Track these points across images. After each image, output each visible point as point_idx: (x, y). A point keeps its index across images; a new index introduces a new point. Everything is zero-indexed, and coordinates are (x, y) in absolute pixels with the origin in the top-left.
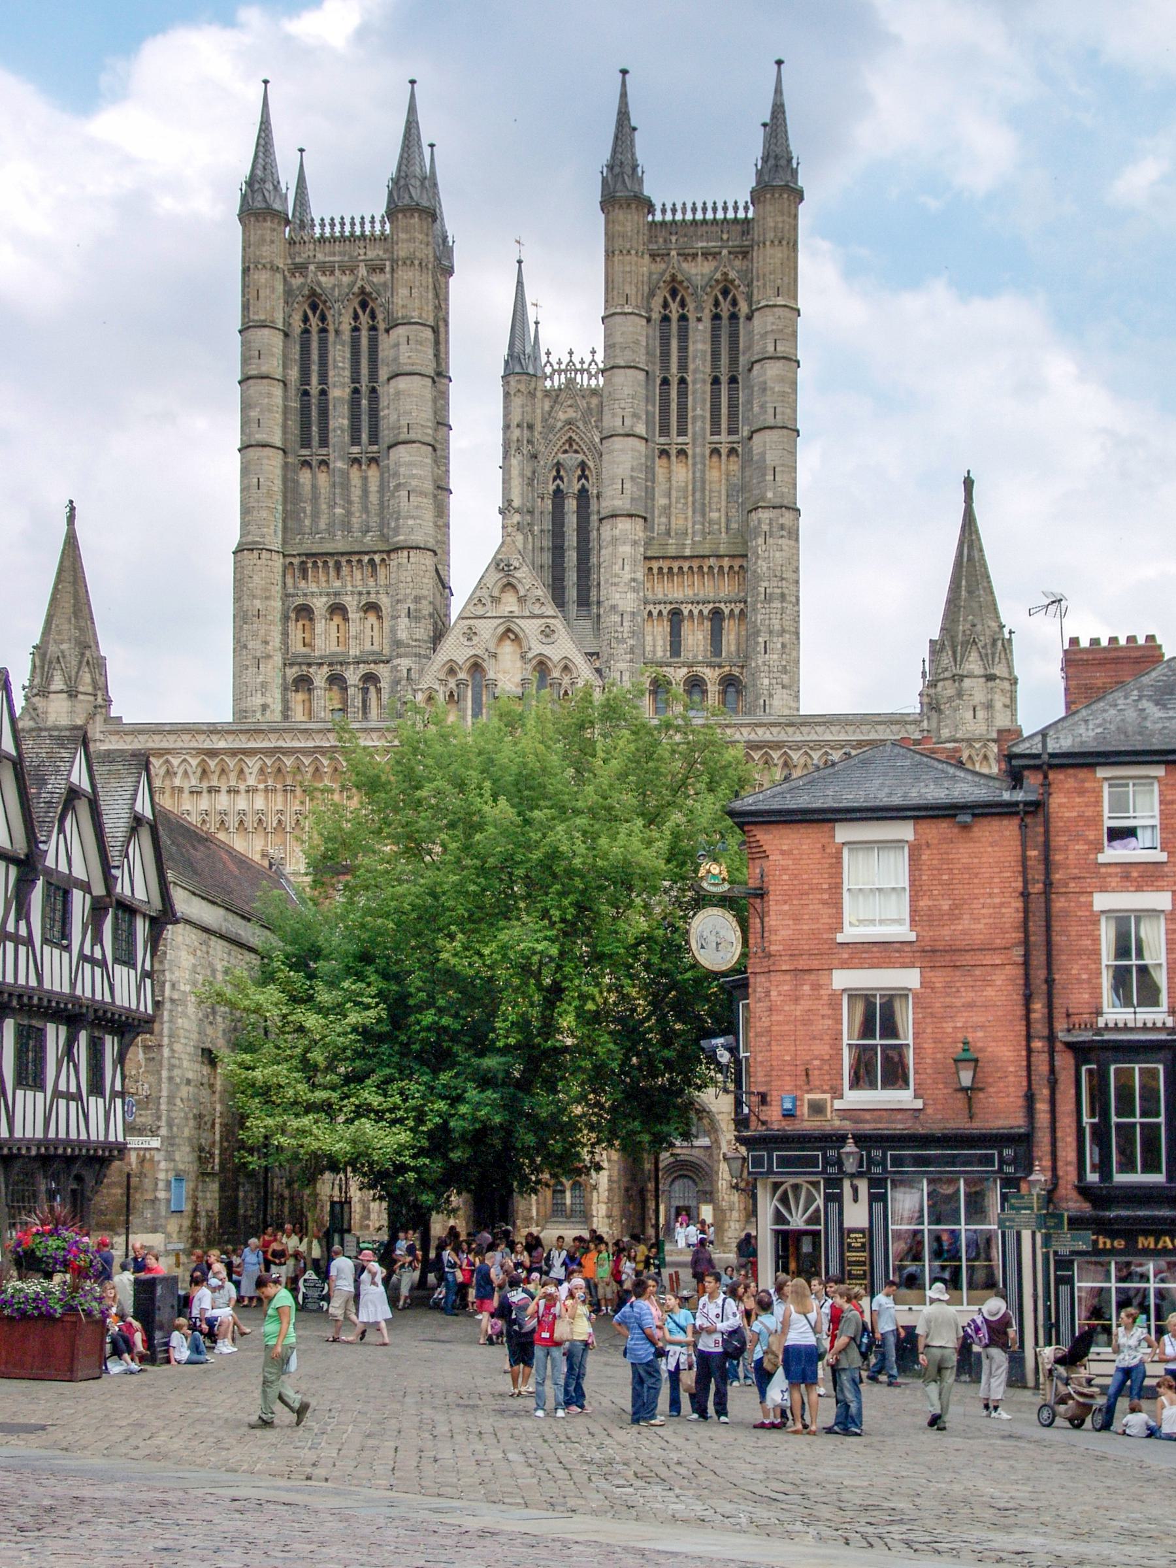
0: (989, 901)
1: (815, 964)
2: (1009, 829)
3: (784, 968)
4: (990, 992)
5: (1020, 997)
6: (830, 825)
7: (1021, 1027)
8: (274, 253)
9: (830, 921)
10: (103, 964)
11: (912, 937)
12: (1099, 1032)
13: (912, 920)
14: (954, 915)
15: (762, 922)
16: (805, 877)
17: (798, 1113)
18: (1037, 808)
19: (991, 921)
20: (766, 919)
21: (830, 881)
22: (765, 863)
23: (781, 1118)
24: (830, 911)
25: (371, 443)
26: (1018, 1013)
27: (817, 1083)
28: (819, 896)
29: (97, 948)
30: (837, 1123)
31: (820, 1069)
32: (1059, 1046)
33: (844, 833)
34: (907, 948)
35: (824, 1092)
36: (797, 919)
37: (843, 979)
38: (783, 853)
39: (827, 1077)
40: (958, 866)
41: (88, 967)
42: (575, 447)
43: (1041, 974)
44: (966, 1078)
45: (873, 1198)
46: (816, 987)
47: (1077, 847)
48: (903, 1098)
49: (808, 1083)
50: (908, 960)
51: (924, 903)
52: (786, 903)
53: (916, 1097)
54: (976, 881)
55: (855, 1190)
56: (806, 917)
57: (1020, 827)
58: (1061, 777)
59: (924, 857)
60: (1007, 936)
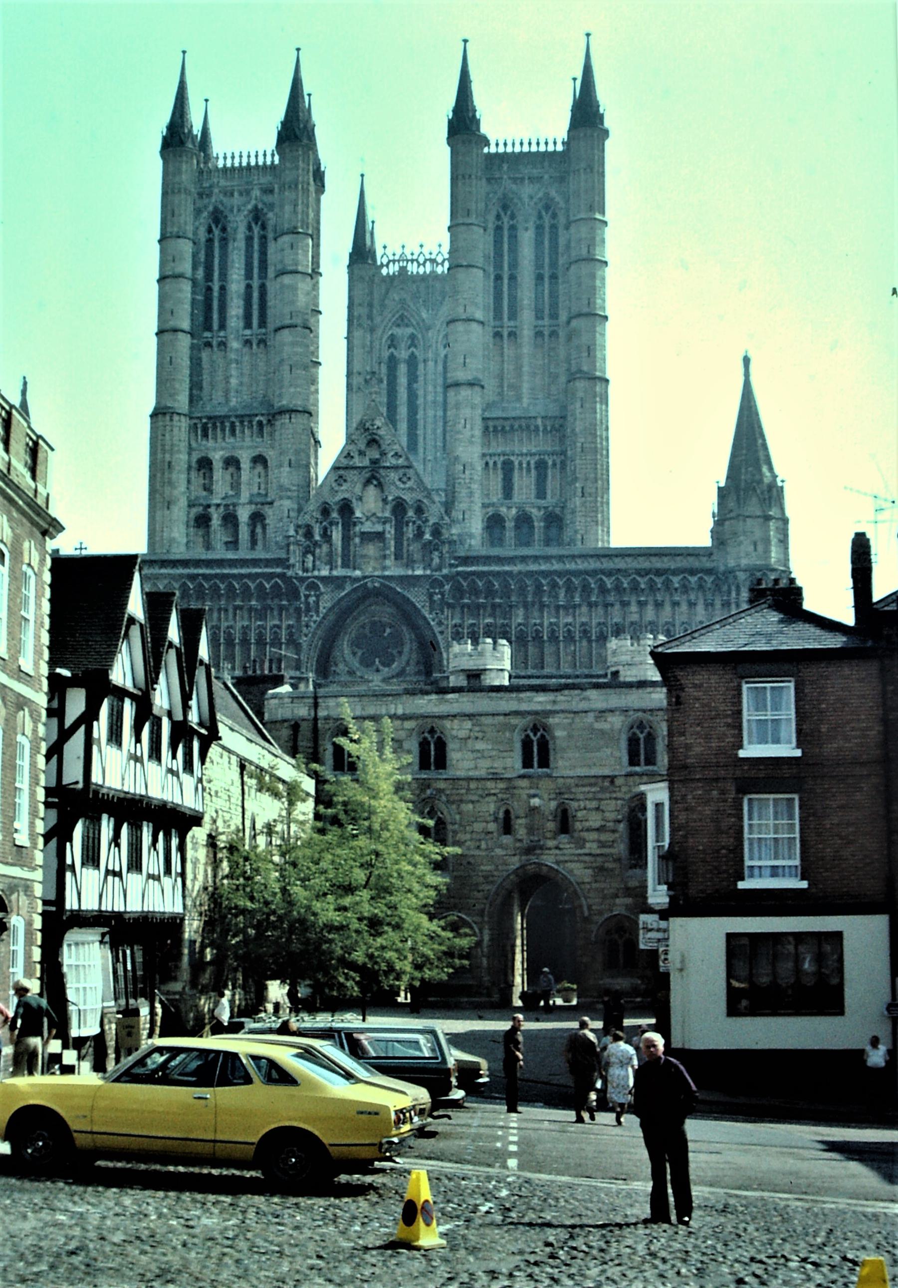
8: (186, 177)
13: (798, 740)
25: (260, 327)
36: (708, 737)
38: (695, 686)
42: (406, 321)
52: (698, 725)
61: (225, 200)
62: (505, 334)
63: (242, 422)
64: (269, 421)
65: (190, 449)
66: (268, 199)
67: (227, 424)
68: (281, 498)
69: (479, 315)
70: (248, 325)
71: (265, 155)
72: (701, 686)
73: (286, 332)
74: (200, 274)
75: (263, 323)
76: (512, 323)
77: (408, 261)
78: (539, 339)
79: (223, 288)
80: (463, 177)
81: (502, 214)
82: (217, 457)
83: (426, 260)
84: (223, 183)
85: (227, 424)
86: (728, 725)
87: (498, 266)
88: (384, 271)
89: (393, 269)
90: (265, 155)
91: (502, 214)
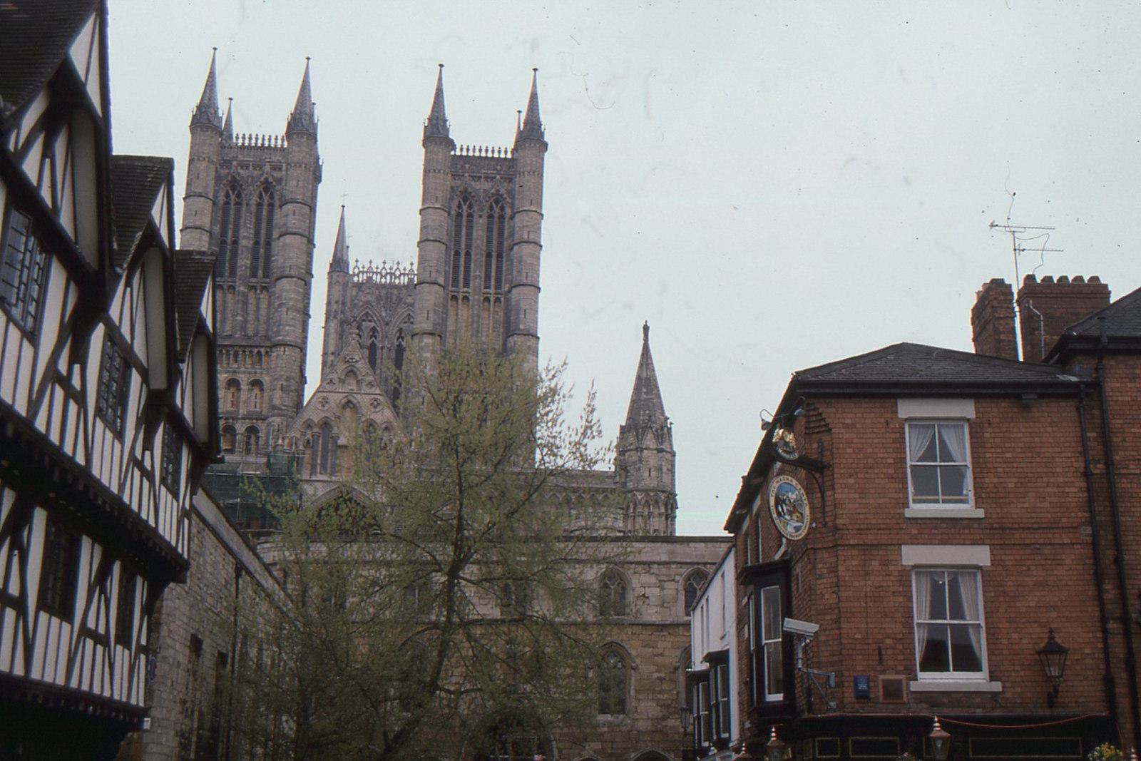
0: (1052, 480)
2: (1066, 410)
3: (852, 542)
5: (1088, 577)
6: (893, 400)
9: (896, 495)
11: (980, 513)
15: (823, 497)
16: (869, 450)
17: (872, 695)
19: (1055, 500)
20: (828, 493)
21: (894, 455)
22: (826, 438)
23: (854, 700)
24: (896, 485)
26: (1090, 593)
27: (891, 663)
28: (885, 471)
31: (893, 649)
33: (906, 409)
34: (975, 526)
35: (898, 673)
37: (912, 555)
38: (846, 426)
39: (901, 657)
40: (1021, 445)
42: (370, 318)
43: (1111, 553)
46: (886, 562)
47: (1133, 430)
48: (975, 680)
49: (881, 661)
50: (978, 537)
51: (989, 480)
52: (851, 476)
53: (993, 678)
54: (1038, 459)
56: (873, 491)
57: (1078, 409)
58: (1113, 363)
59: (987, 435)
60: (1073, 515)
61: (241, 172)
62: (460, 297)
63: (244, 352)
64: (267, 352)
66: (277, 174)
67: (232, 352)
68: (274, 415)
69: (441, 281)
70: (254, 275)
71: (276, 139)
72: (854, 425)
73: (284, 280)
74: (217, 229)
76: (465, 289)
77: (373, 273)
78: (486, 304)
79: (235, 242)
80: (434, 170)
81: (462, 203)
83: (387, 273)
84: (241, 157)
85: (232, 352)
86: (890, 477)
87: (458, 243)
88: (356, 279)
89: (362, 278)
90: (276, 139)
91: (462, 203)
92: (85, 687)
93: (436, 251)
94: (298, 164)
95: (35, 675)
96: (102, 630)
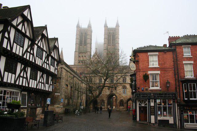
1: (146, 70)
2: (171, 53)
4: (170, 74)
7: (174, 79)
10: (49, 64)
11: (159, 67)
12: (185, 79)
14: (164, 64)
18: (175, 50)
22: (138, 58)
29: (48, 62)
30: (149, 91)
32: (180, 81)
33: (149, 54)
36: (143, 64)
41: (46, 64)
43: (177, 72)
44: (168, 85)
45: (154, 102)
48: (158, 88)
53: (160, 88)
55: (152, 101)
65: (78, 55)
75: (86, 44)
82: (81, 56)
92: (40, 88)
93: (106, 40)
94: (89, 31)
95: (30, 86)
96: (43, 82)
